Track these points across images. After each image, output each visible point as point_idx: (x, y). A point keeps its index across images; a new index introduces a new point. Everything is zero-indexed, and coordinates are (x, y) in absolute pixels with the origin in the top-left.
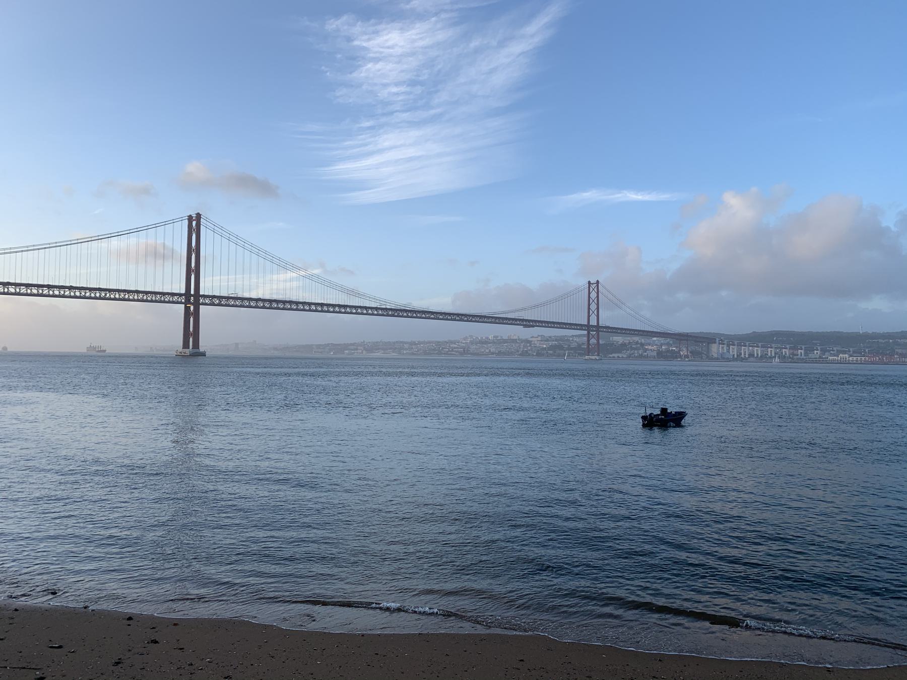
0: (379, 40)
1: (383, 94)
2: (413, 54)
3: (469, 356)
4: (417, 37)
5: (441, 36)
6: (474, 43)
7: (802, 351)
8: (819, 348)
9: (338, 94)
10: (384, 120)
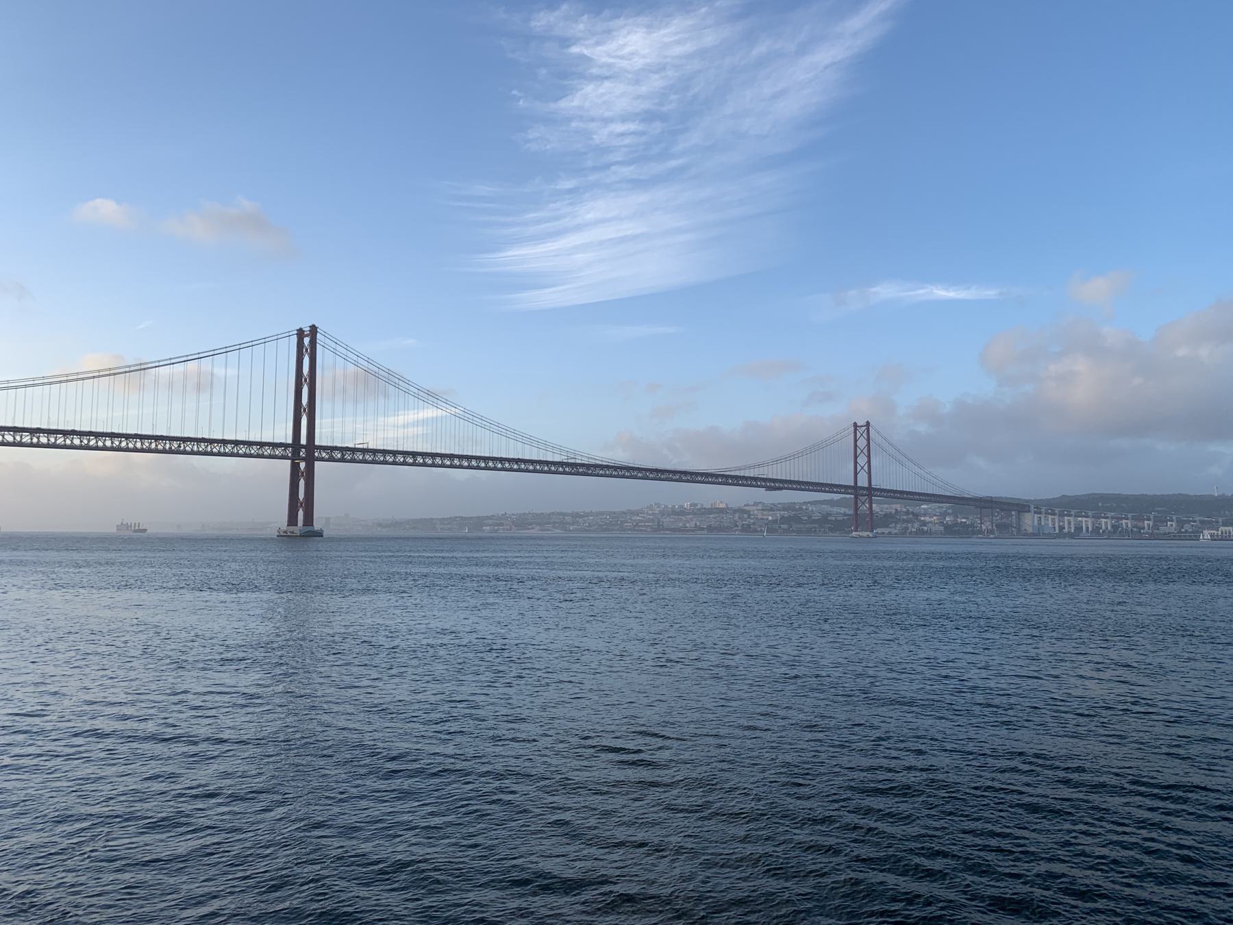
0: (610, 46)
1: (601, 135)
2: (660, 68)
4: (672, 39)
5: (710, 39)
6: (761, 48)
7: (1151, 523)
8: (1174, 518)
9: (532, 134)
10: (593, 178)
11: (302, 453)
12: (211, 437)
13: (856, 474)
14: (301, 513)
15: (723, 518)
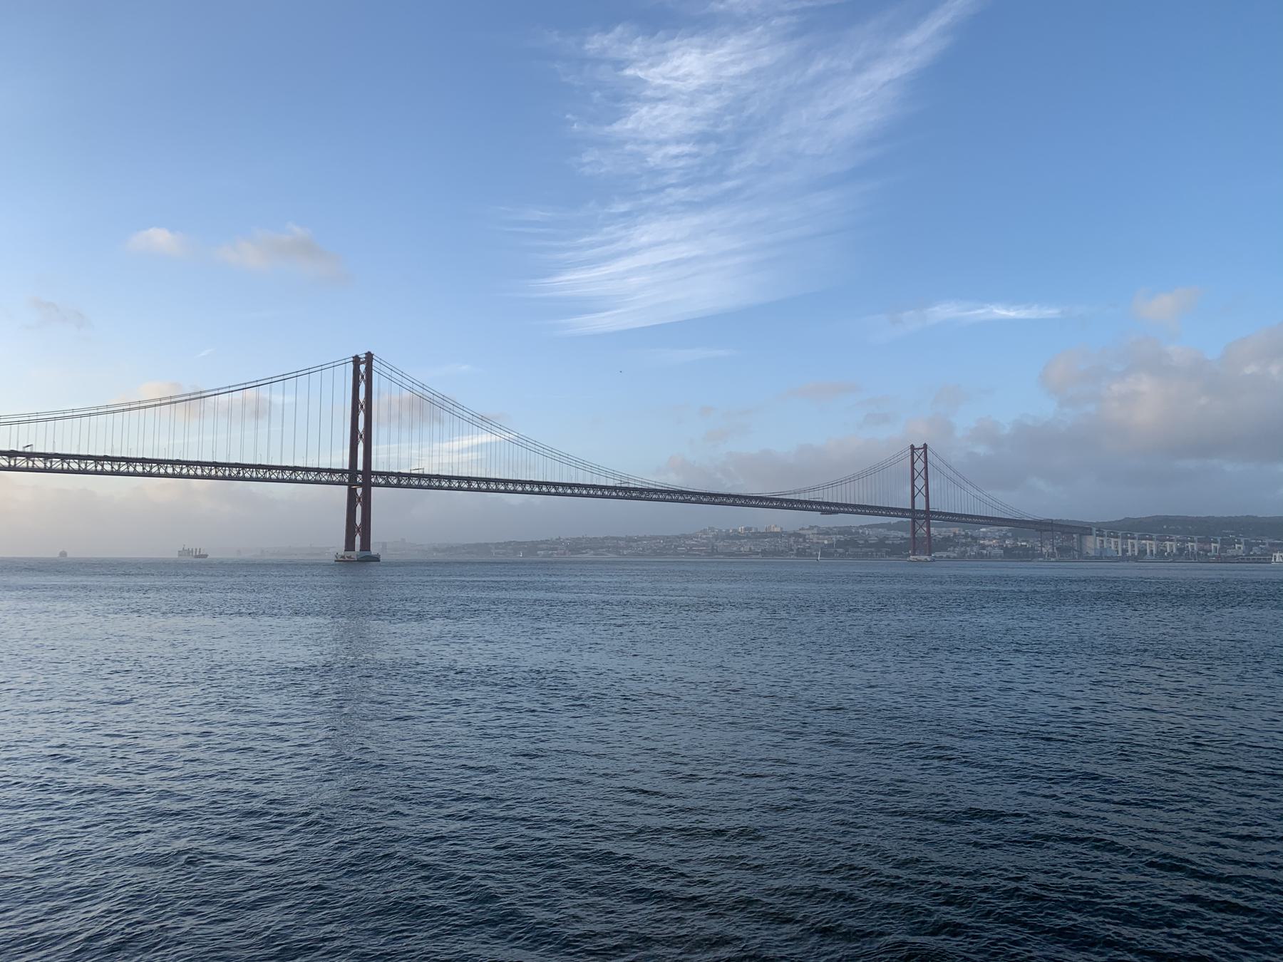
0: (665, 68)
1: (656, 158)
2: (716, 89)
3: (722, 557)
7: (1218, 546)
8: (1242, 540)
9: (586, 159)
10: (647, 200)
11: (359, 480)
12: (270, 464)
13: (913, 497)
14: (358, 538)
15: (778, 542)
